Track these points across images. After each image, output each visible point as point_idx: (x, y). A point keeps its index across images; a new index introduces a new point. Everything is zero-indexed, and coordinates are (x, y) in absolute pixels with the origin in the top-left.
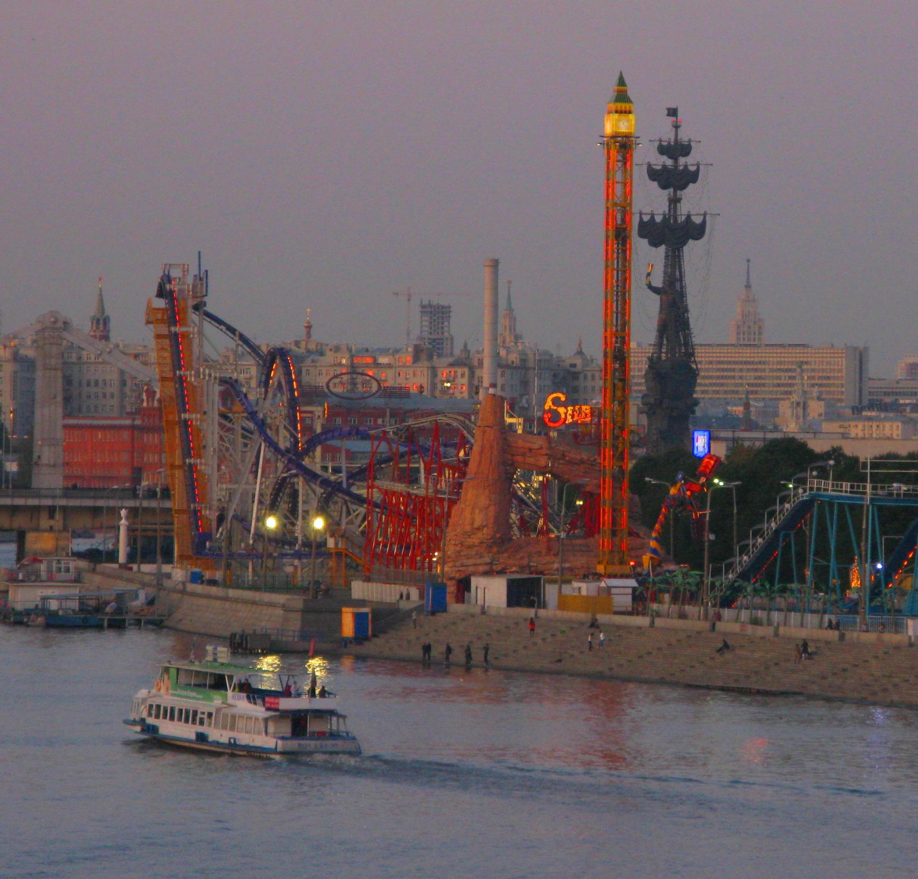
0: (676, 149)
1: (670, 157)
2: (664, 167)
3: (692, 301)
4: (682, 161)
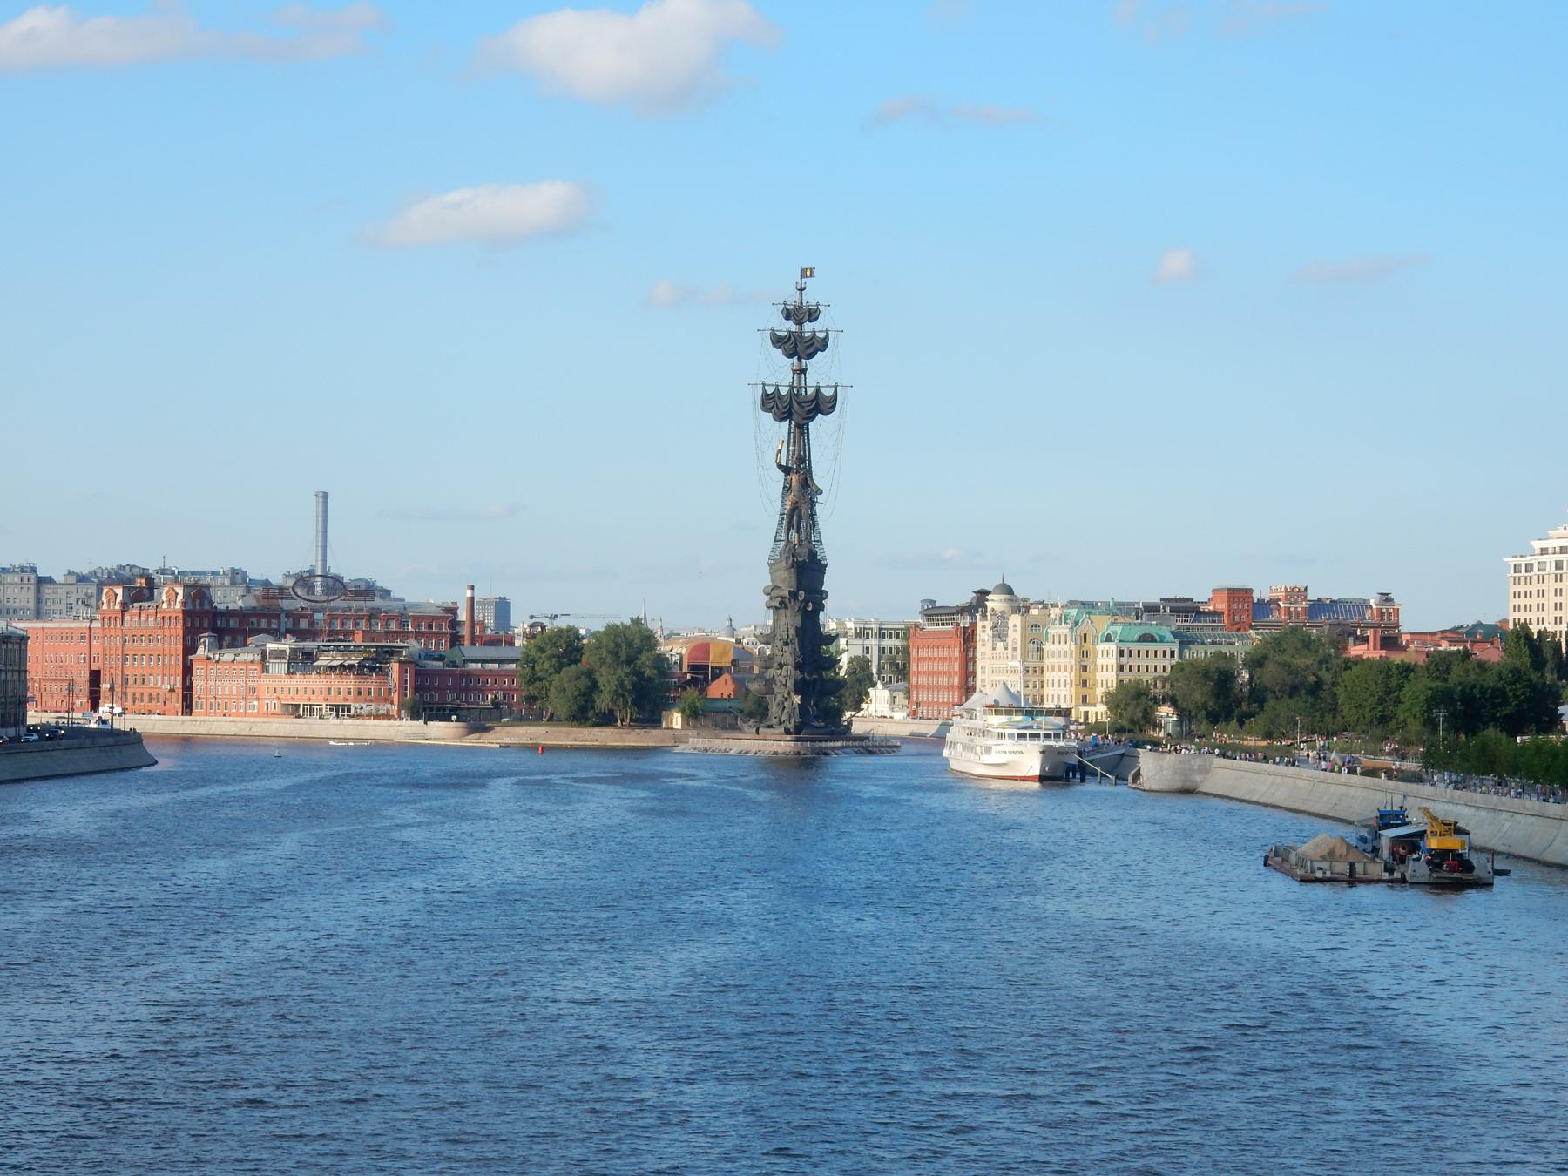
4: (808, 327)
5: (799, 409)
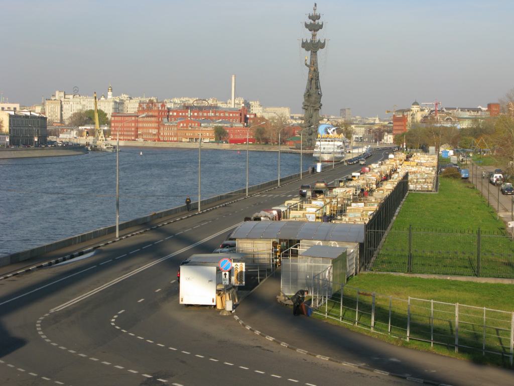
0: (315, 17)
1: (313, 20)
2: (311, 23)
3: (320, 70)
4: (317, 21)
5: (313, 47)
